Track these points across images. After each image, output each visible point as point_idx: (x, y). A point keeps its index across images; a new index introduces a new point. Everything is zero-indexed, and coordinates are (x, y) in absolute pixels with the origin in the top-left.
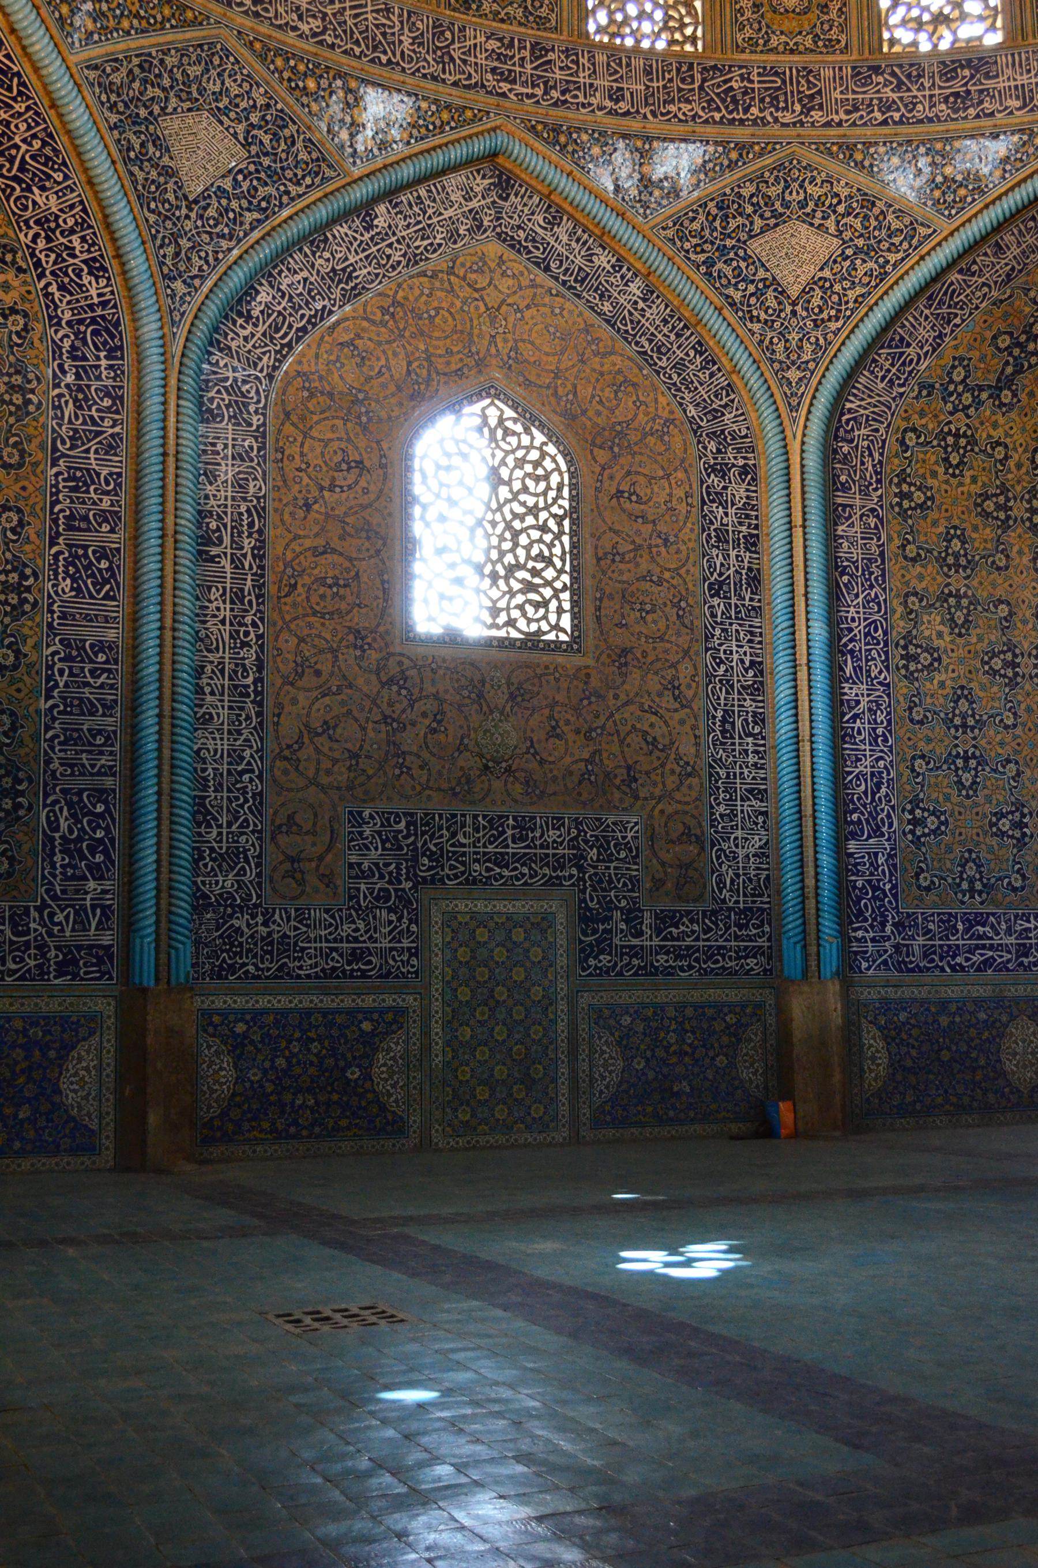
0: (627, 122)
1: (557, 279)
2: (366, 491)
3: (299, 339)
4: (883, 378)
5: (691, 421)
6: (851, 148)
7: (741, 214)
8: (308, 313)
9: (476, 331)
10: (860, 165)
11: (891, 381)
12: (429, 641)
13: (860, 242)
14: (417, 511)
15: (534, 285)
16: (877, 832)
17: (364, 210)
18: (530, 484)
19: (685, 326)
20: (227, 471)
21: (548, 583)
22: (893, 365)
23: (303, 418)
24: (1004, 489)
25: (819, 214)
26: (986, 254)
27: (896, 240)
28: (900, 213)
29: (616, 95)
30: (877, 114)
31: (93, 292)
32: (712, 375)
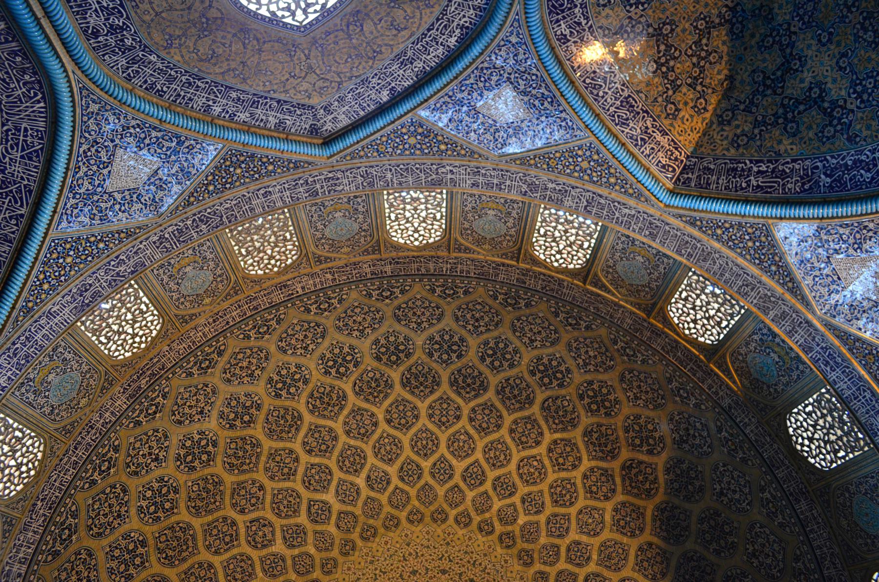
0: (257, 187)
1: (271, 99)
3: (433, 25)
4: (26, 130)
5: (151, 52)
6: (128, 236)
7: (174, 175)
8: (427, 39)
9: (320, 58)
11: (19, 131)
13: (95, 198)
15: (286, 92)
19: (175, 101)
22: (26, 141)
25: (128, 197)
26: (13, 233)
27: (75, 211)
30: (124, 257)
31: (563, 26)
32: (146, 82)
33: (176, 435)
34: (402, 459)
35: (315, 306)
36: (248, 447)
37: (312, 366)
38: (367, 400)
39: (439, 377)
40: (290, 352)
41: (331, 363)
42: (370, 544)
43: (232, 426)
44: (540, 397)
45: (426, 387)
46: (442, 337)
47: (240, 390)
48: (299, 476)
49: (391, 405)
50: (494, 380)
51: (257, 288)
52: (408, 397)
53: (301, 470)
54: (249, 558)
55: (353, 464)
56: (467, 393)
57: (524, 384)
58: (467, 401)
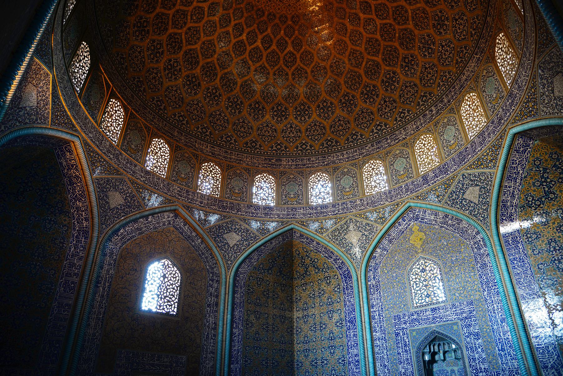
2: (136, 276)
5: (207, 269)
10: (246, 223)
12: (144, 311)
14: (147, 282)
15: (179, 237)
16: (237, 363)
17: (147, 217)
18: (172, 279)
20: (106, 267)
21: (173, 301)
23: (125, 258)
24: (268, 290)
28: (253, 234)
29: (201, 203)
33: (280, 127)
34: (223, 30)
35: (208, 133)
36: (265, 94)
37: (223, 103)
38: (215, 68)
39: (183, 56)
40: (226, 118)
41: (216, 98)
42: (264, 8)
43: (263, 108)
44: (152, 16)
45: (191, 55)
46: (171, 77)
47: (250, 119)
48: (261, 63)
49: (209, 58)
50: (164, 38)
51: (221, 161)
52: (200, 56)
53: (258, 65)
54: (301, 57)
55: (240, 47)
56: (178, 38)
57: (154, 27)
58: (180, 34)
